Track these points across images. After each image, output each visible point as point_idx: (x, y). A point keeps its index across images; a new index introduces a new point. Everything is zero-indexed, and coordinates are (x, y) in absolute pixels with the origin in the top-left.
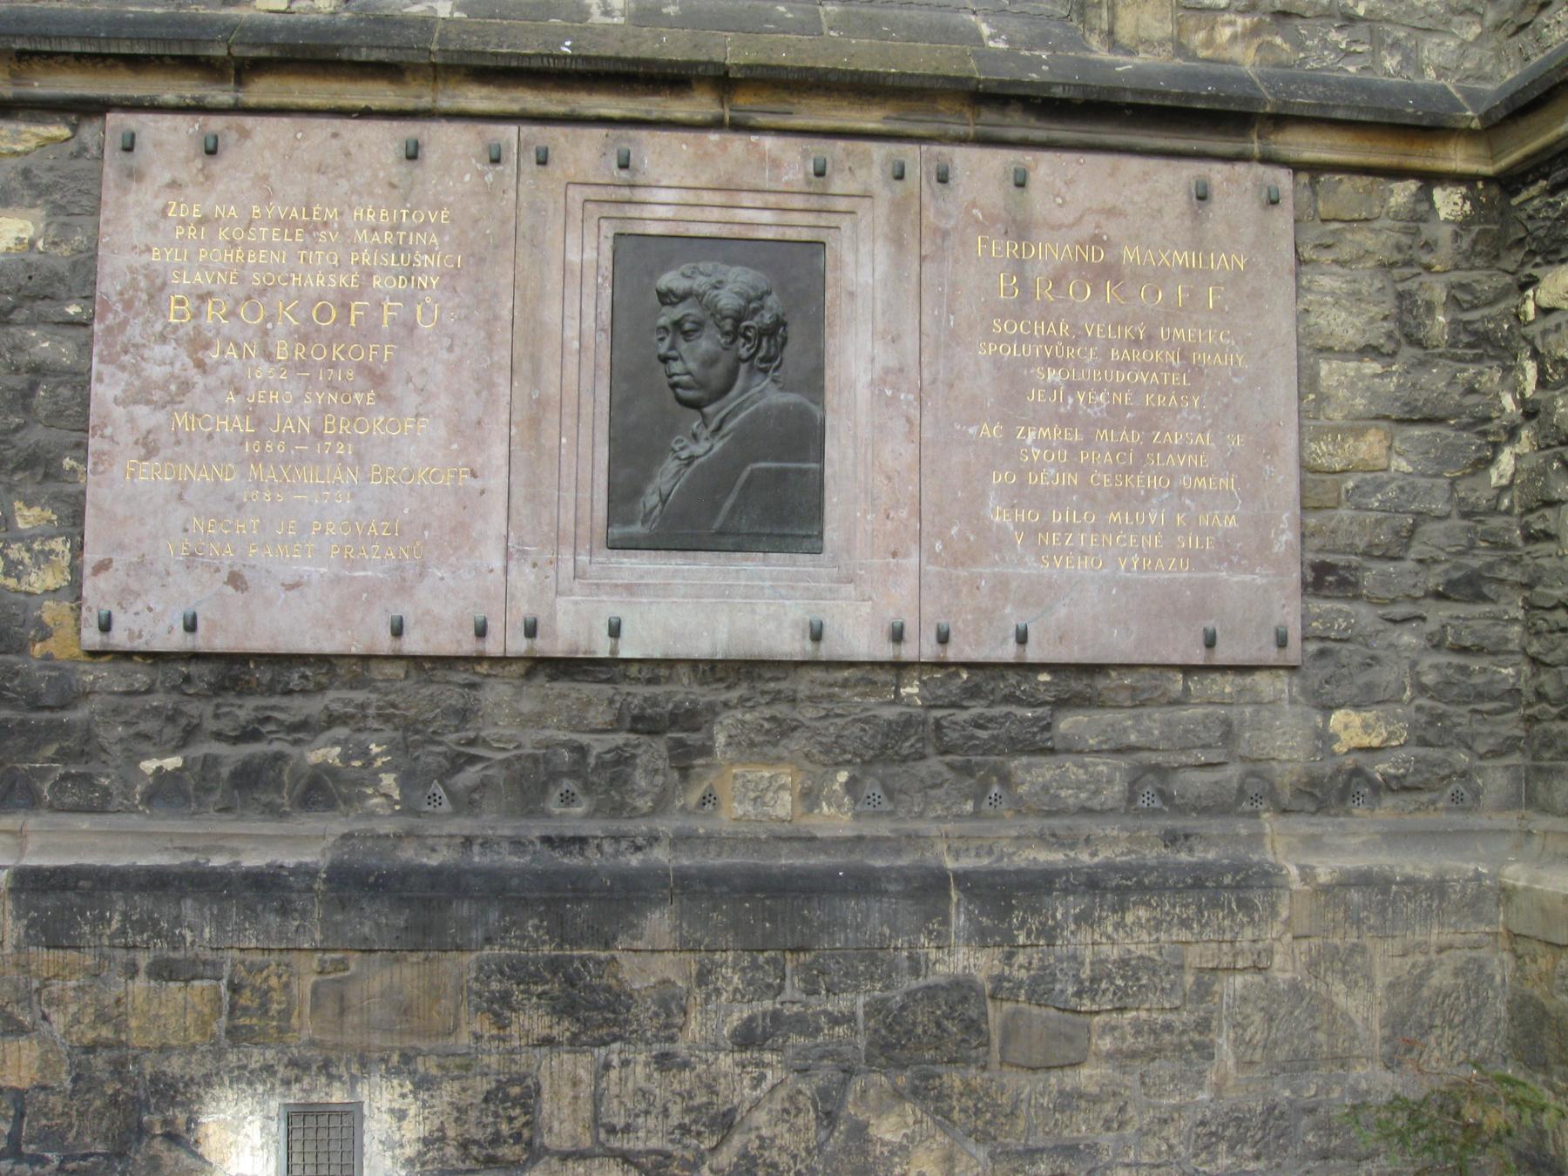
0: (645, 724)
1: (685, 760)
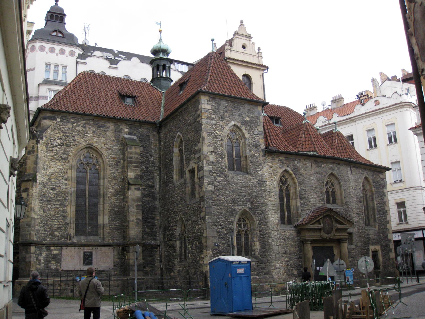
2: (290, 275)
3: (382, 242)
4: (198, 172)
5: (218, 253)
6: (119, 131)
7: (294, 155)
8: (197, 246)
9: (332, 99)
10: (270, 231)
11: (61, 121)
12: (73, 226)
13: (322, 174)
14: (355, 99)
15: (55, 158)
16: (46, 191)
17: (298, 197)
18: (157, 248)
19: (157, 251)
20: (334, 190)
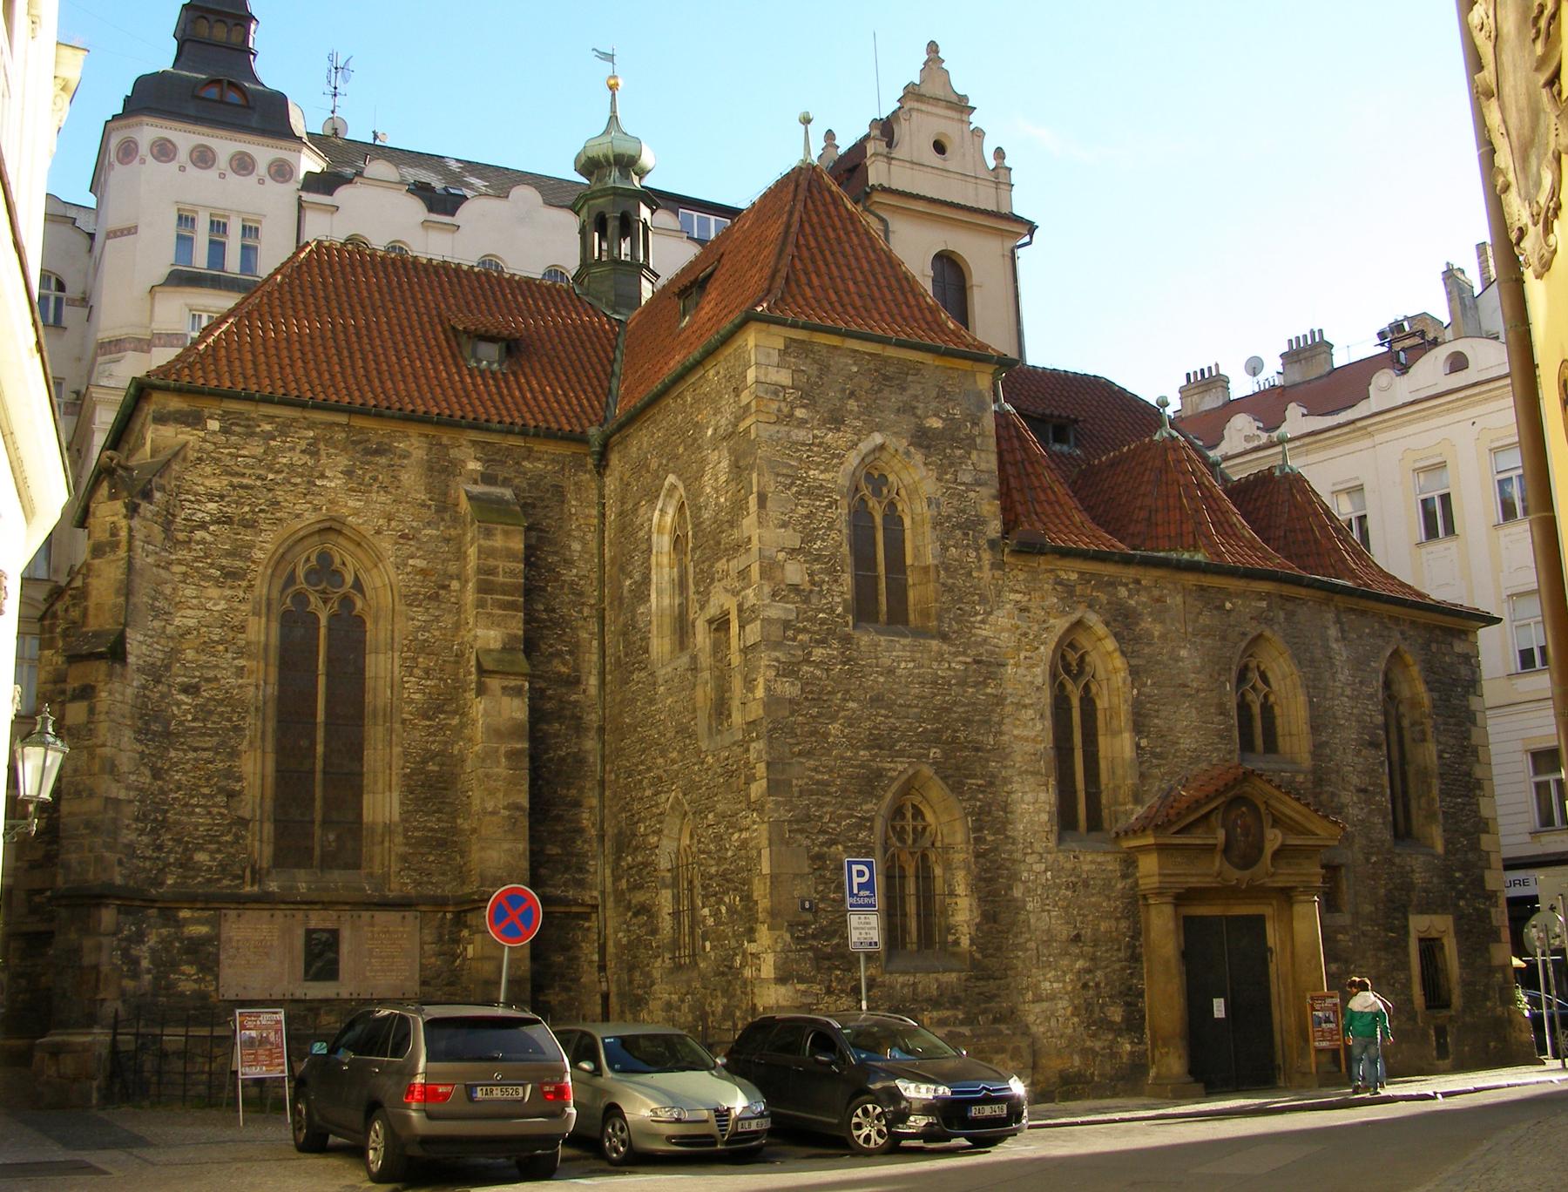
0: (310, 1010)
1: (317, 1015)
2: (1094, 1023)
3: (1462, 903)
4: (742, 627)
5: (814, 937)
6: (444, 470)
7: (1117, 562)
8: (736, 912)
9: (1286, 349)
10: (1018, 856)
11: (225, 431)
12: (268, 828)
14: (1370, 348)
15: (197, 569)
16: (163, 696)
18: (587, 917)
19: (588, 929)
20: (1272, 699)
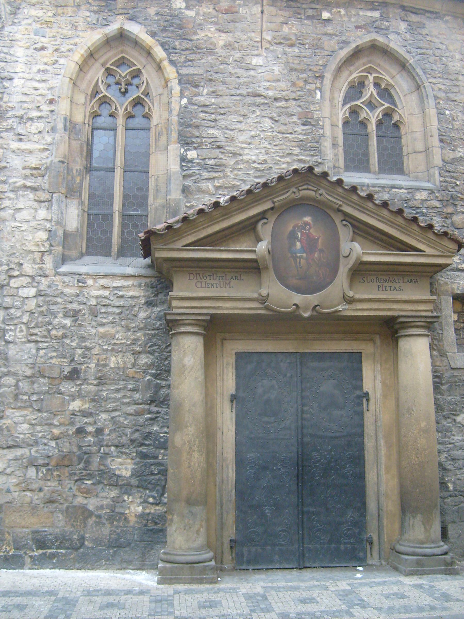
2: (90, 476)
13: (316, 47)
17: (174, 135)
20: (396, 118)
